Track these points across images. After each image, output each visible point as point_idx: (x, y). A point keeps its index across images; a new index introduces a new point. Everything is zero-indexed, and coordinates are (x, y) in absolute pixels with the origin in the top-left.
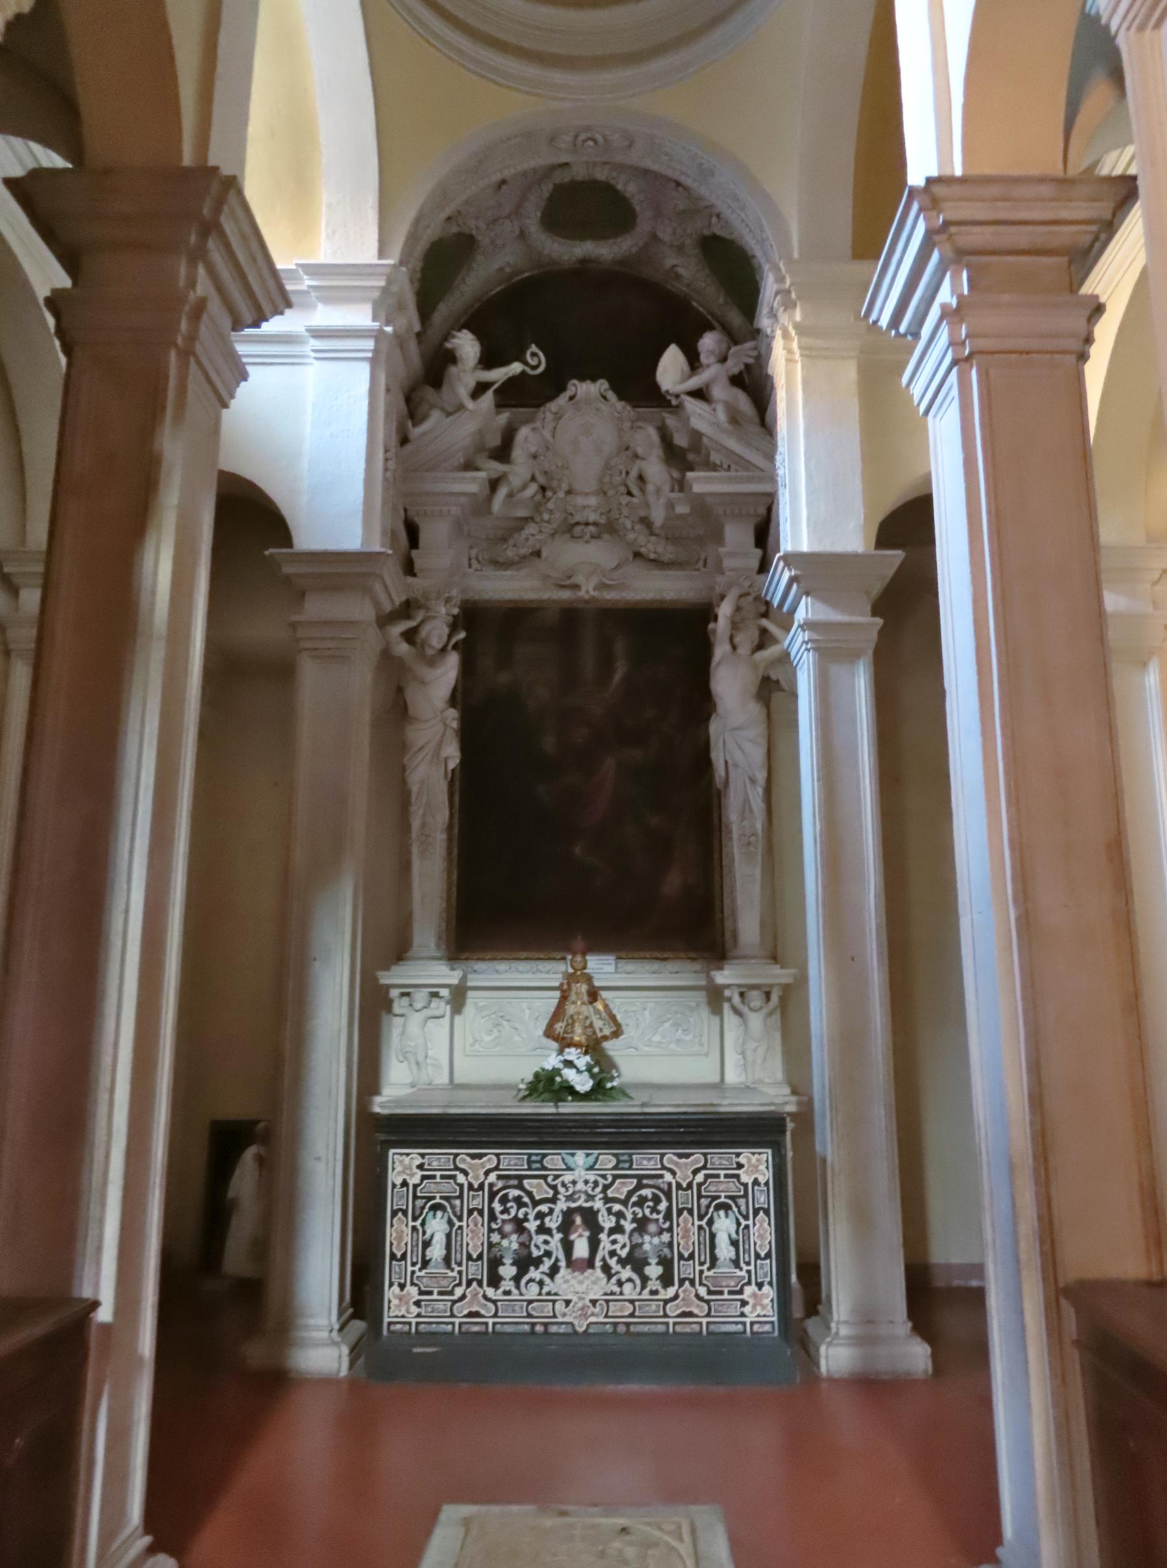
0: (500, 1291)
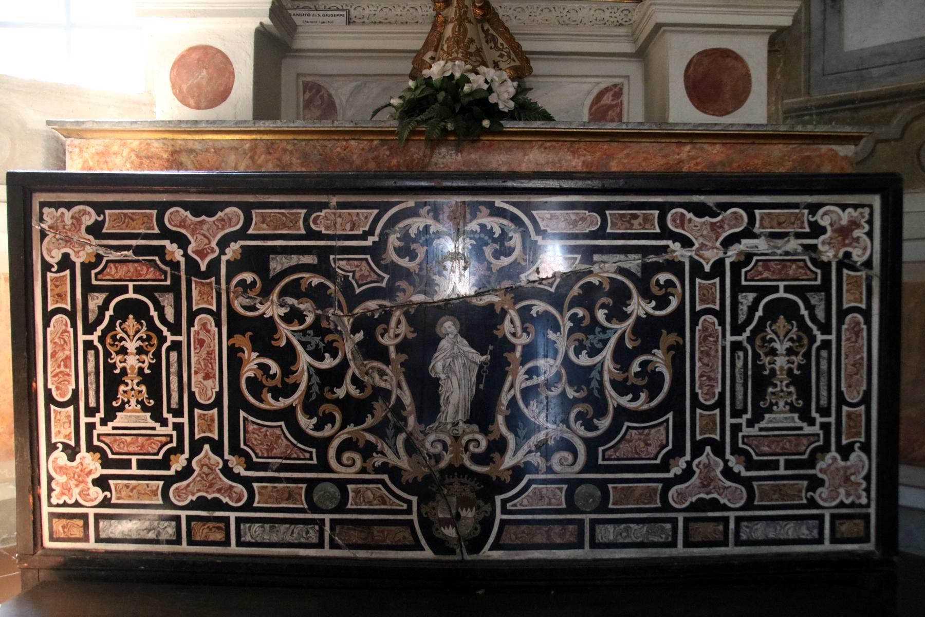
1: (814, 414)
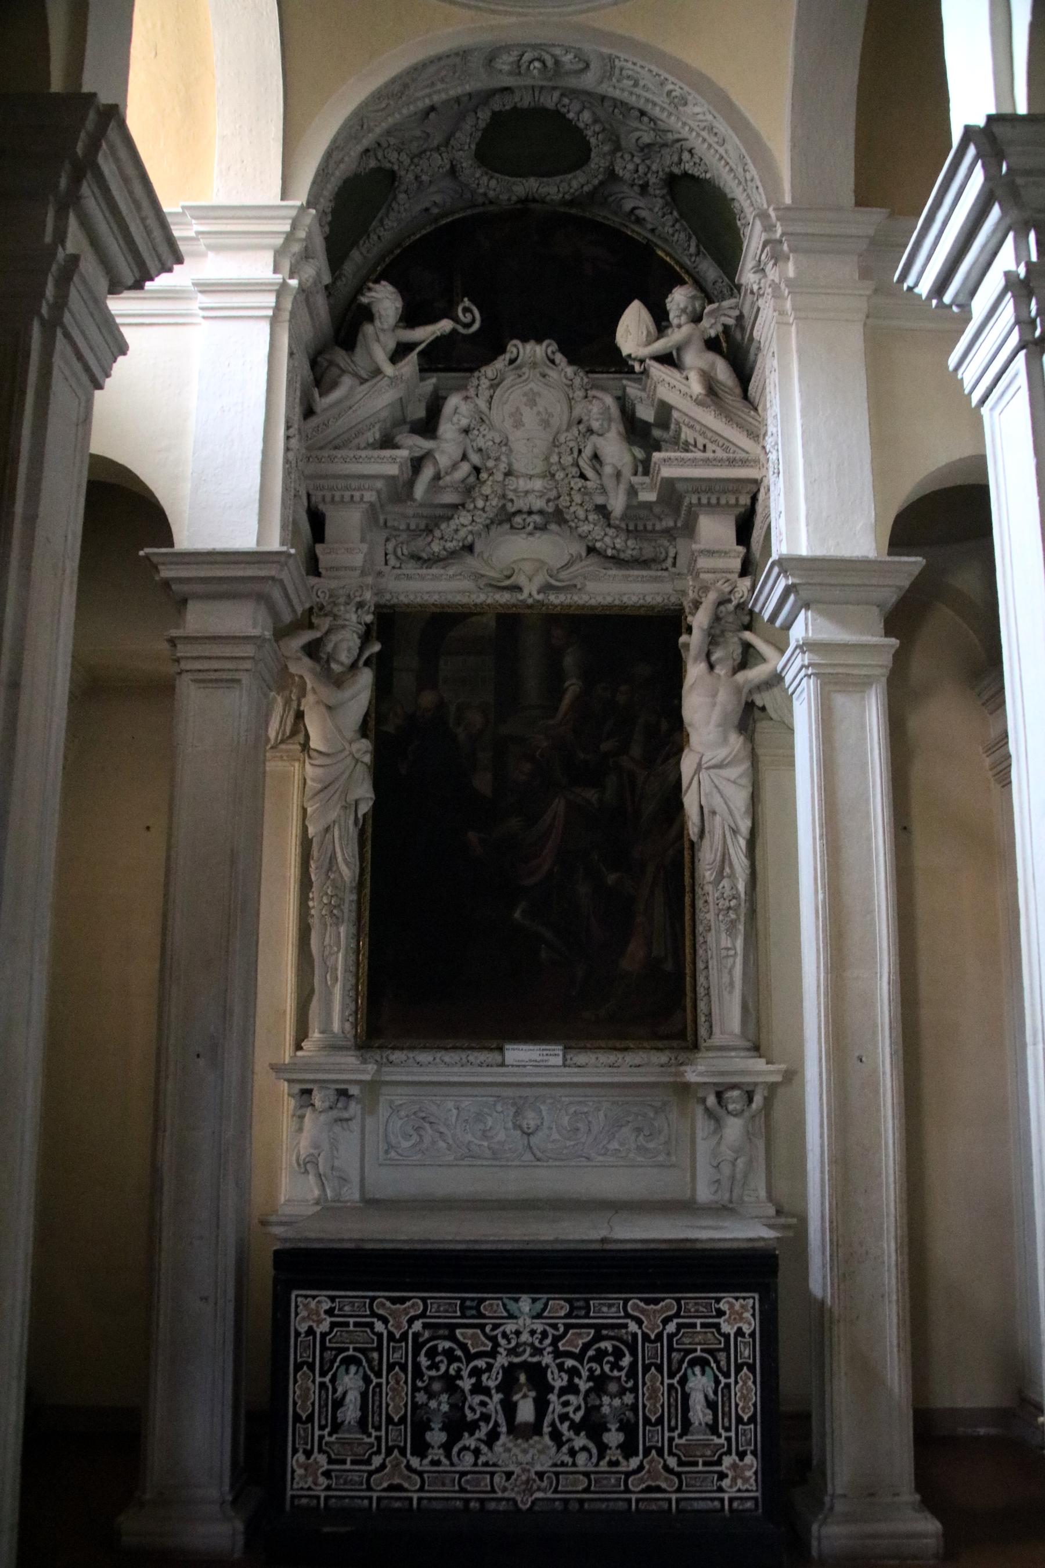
0: (426, 1461)
1: (721, 1430)
